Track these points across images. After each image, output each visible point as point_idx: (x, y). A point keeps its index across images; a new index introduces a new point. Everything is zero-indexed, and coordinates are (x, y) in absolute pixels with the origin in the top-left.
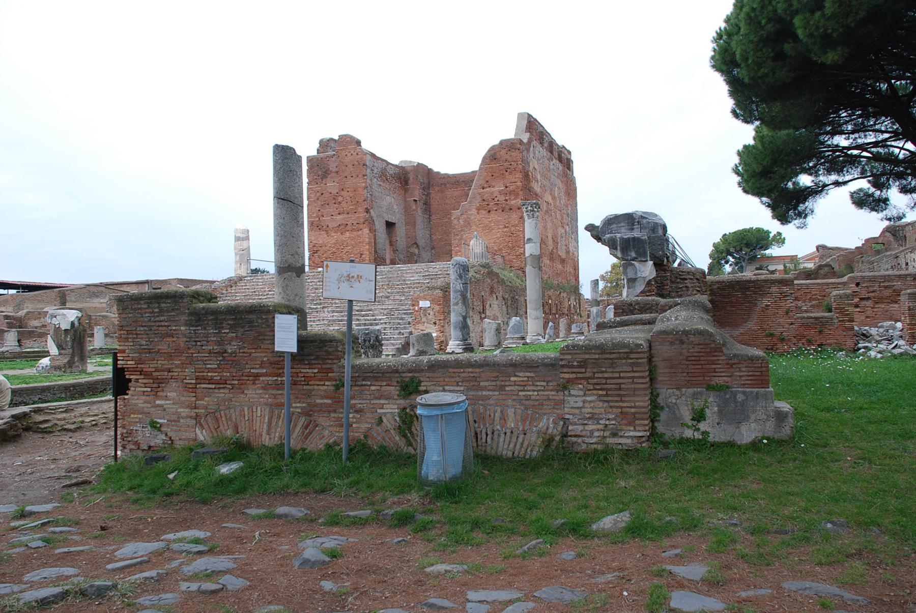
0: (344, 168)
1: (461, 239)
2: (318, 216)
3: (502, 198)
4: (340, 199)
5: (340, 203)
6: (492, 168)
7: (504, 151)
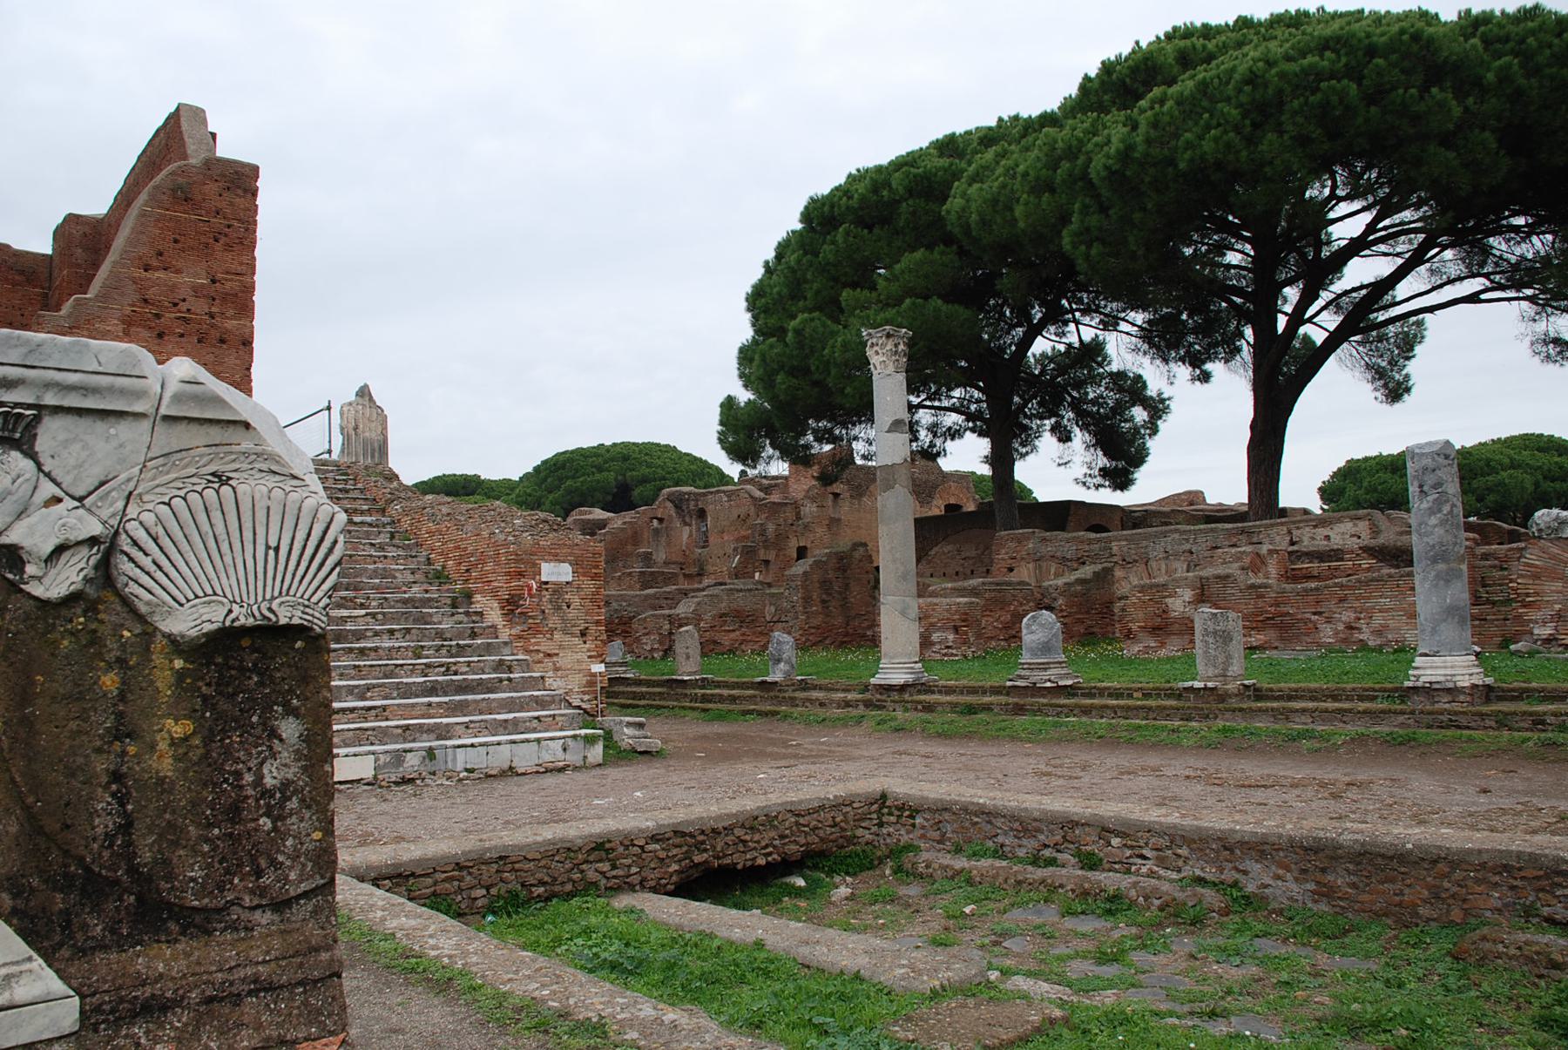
3: (200, 307)
6: (177, 220)
7: (212, 188)
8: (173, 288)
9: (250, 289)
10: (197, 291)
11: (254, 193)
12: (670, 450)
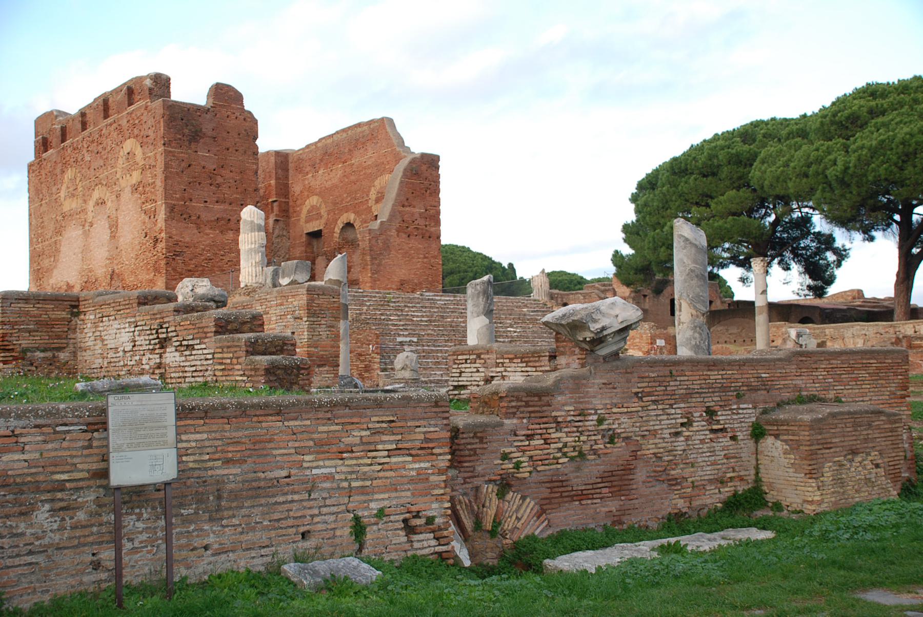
0: (225, 134)
1: (379, 265)
2: (183, 199)
3: (422, 222)
4: (219, 180)
5: (218, 186)
7: (424, 167)
8: (413, 214)
9: (438, 213)
10: (421, 214)
11: (438, 168)
12: (465, 250)
